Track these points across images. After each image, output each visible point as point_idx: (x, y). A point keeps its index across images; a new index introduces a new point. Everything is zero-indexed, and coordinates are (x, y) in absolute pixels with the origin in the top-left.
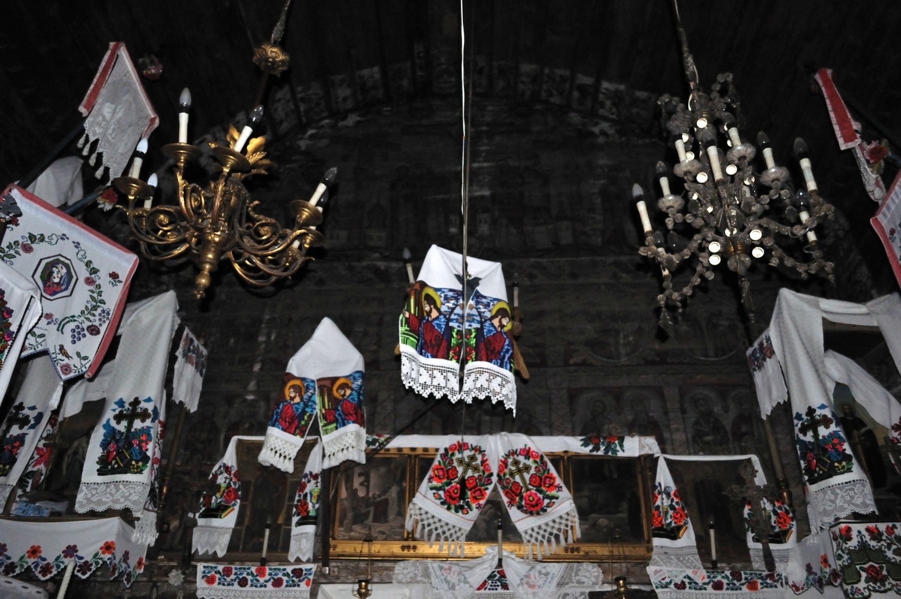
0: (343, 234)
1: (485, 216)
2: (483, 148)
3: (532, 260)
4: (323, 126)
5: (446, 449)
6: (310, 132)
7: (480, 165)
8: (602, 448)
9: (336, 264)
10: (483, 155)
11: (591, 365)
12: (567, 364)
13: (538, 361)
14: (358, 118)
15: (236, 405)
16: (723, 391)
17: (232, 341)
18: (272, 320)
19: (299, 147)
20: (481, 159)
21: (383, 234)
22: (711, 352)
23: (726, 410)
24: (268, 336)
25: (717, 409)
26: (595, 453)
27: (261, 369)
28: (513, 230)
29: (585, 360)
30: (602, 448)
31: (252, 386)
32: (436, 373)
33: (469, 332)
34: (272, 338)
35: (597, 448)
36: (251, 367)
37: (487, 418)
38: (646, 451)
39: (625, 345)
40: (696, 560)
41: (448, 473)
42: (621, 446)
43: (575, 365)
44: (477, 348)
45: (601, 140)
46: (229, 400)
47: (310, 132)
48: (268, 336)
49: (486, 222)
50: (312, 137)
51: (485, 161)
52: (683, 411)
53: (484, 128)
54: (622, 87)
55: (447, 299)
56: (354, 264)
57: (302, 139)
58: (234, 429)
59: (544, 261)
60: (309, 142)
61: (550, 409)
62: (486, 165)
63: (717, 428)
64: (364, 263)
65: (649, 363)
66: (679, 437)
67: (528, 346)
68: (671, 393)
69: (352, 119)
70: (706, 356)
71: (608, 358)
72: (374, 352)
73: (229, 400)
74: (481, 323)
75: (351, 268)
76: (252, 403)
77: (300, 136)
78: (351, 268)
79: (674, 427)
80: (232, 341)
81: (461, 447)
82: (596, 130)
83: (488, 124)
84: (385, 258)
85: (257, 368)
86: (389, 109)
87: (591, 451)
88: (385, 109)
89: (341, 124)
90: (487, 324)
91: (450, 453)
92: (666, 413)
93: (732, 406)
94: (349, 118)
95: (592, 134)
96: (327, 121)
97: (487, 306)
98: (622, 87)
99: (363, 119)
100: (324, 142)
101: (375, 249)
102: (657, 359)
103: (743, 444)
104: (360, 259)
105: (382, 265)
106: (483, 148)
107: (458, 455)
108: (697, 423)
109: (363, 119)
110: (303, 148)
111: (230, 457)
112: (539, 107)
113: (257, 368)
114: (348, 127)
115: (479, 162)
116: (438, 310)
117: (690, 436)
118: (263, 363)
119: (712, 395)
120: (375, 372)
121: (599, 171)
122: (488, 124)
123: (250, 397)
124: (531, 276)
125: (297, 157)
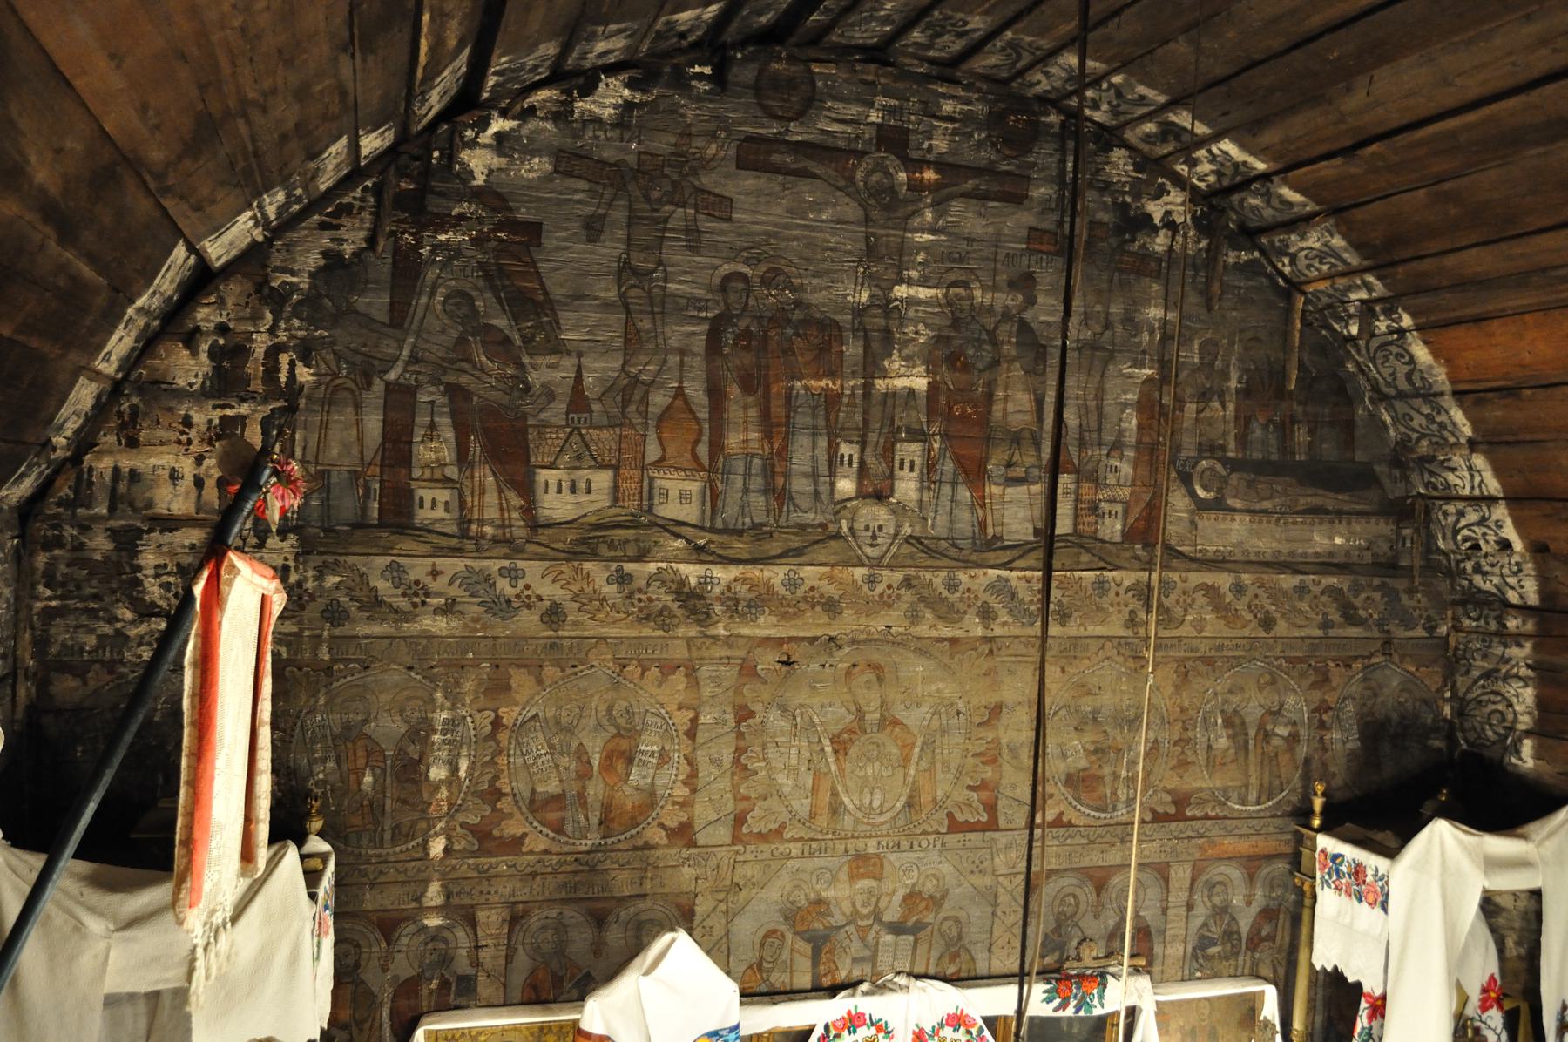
0: (602, 480)
1: (910, 451)
4: (532, 111)
5: (827, 1027)
6: (498, 125)
7: (913, 291)
8: (1073, 1003)
9: (587, 566)
11: (1070, 824)
13: (985, 818)
14: (627, 93)
15: (404, 940)
17: (368, 779)
21: (694, 487)
22: (1253, 796)
26: (1060, 1013)
27: (447, 851)
28: (964, 494)
29: (1062, 813)
30: (1073, 1003)
34: (462, 773)
35: (1063, 1006)
36: (425, 846)
37: (889, 938)
42: (1101, 997)
45: (1160, 242)
46: (388, 926)
47: (498, 125)
50: (499, 136)
51: (924, 282)
53: (930, 175)
56: (629, 567)
57: (473, 144)
61: (994, 914)
62: (923, 293)
66: (1175, 950)
67: (970, 788)
68: (1180, 874)
70: (1244, 802)
71: (1097, 809)
72: (684, 804)
73: (388, 926)
75: (623, 579)
76: (436, 935)
78: (623, 579)
80: (368, 779)
82: (1156, 210)
83: (940, 165)
84: (699, 553)
85: (437, 847)
86: (707, 70)
87: (1055, 1010)
91: (833, 1032)
92: (1164, 911)
93: (1259, 892)
95: (1145, 223)
96: (544, 94)
99: (638, 97)
100: (539, 165)
101: (673, 528)
102: (1172, 810)
103: (1257, 956)
104: (640, 558)
105: (691, 572)
109: (638, 97)
110: (480, 180)
112: (1053, 118)
114: (597, 121)
117: (1189, 949)
120: (686, 853)
121: (1145, 336)
122: (940, 165)
123: (433, 921)
124: (986, 614)
125: (464, 207)
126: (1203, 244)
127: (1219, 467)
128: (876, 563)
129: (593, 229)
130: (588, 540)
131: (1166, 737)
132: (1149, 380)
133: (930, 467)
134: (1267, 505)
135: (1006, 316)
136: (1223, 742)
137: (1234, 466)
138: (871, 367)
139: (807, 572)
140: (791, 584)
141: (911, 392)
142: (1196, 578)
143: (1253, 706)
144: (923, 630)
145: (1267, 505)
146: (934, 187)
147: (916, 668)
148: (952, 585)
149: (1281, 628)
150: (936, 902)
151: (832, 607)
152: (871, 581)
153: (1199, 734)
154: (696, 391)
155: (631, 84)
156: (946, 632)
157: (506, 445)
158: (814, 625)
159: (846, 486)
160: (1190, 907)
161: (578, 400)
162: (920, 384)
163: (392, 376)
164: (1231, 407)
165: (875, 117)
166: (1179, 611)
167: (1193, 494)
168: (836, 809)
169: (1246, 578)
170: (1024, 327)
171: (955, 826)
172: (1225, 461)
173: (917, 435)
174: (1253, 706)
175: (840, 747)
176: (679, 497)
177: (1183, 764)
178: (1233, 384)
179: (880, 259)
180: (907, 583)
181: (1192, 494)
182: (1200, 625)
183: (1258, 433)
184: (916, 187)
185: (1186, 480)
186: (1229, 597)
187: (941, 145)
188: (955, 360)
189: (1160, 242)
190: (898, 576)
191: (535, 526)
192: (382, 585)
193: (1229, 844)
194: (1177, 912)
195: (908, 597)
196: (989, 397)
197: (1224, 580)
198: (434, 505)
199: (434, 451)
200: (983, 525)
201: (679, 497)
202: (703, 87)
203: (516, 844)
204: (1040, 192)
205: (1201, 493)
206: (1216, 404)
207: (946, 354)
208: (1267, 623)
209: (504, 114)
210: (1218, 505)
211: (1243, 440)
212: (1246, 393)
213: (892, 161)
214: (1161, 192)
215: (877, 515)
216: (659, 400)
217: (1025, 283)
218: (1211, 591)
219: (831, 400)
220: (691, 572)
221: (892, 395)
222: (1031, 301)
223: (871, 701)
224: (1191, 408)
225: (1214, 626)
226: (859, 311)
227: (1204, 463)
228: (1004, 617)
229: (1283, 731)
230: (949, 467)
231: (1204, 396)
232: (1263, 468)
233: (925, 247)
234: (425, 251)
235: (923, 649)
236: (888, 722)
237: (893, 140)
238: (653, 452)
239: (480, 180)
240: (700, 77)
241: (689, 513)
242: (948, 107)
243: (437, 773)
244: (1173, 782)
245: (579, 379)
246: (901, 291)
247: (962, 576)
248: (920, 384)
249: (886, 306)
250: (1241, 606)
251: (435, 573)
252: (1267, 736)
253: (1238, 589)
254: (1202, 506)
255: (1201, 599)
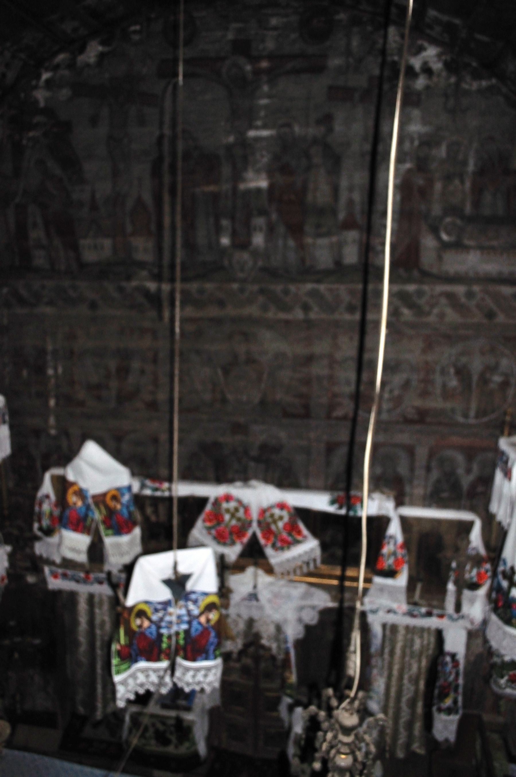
0: (107, 243)
1: (260, 221)
2: (264, 102)
3: (309, 286)
6: (45, 76)
10: (262, 113)
12: (329, 417)
16: (470, 453)
18: (55, 352)
19: (37, 102)
20: (259, 123)
22: (472, 413)
23: (469, 471)
24: (56, 369)
25: (460, 471)
28: (291, 243)
31: (52, 421)
32: (151, 673)
33: (177, 634)
36: (47, 402)
38: (383, 512)
39: (390, 400)
40: (403, 597)
41: (216, 517)
43: (338, 418)
44: (185, 649)
46: (37, 433)
47: (45, 76)
48: (56, 369)
49: (261, 230)
50: (48, 82)
51: (265, 127)
52: (428, 469)
53: (264, 64)
54: (457, 21)
55: (156, 610)
57: (36, 87)
58: (45, 469)
59: (322, 287)
60: (48, 94)
62: (265, 133)
63: (455, 486)
64: (134, 283)
65: (408, 421)
66: (419, 491)
69: (93, 51)
74: (189, 623)
75: (121, 290)
77: (34, 83)
78: (121, 290)
79: (416, 482)
81: (228, 498)
82: (416, 63)
83: (270, 57)
85: (52, 402)
86: (138, 28)
88: (133, 28)
89: (81, 59)
90: (195, 623)
93: (475, 467)
94: (88, 49)
97: (195, 602)
98: (457, 21)
99: (106, 49)
100: (65, 93)
101: (142, 265)
104: (129, 278)
105: (152, 286)
106: (264, 102)
107: (225, 505)
108: (438, 481)
109: (106, 49)
110: (42, 104)
111: (47, 487)
113: (52, 402)
114: (88, 65)
115: (257, 128)
116: (149, 619)
118: (57, 398)
119: (460, 458)
122: (270, 57)
124: (306, 308)
126: (453, 80)
127: (459, 222)
128: (244, 281)
129: (94, 121)
130: (103, 272)
131: (415, 378)
132: (409, 171)
133: (271, 230)
134: (495, 243)
135: (315, 141)
136: (454, 383)
137: (470, 220)
138: (237, 177)
139: (209, 286)
140: (201, 291)
141: (259, 190)
142: (440, 288)
143: (477, 365)
144: (270, 315)
145: (495, 243)
146: (269, 71)
147: (266, 335)
148: (286, 292)
149: (501, 318)
150: (277, 449)
151: (221, 304)
152: (242, 290)
153: (438, 379)
154: (147, 198)
155: (103, 43)
156: (282, 316)
157: (65, 229)
158: (214, 312)
159: (225, 241)
160: (428, 469)
161: (94, 207)
162: (263, 184)
163: (17, 200)
164: (468, 185)
165: (230, 36)
166: (427, 308)
167: (438, 238)
168: (224, 401)
169: (476, 288)
170: (327, 147)
171: (286, 414)
172: (462, 217)
173: (263, 212)
174: (477, 365)
175: (226, 372)
176: (143, 248)
177: (424, 394)
178: (471, 167)
179: (243, 116)
180: (262, 291)
181: (438, 238)
182: (442, 316)
183: (487, 198)
184: (257, 72)
185: (435, 230)
186: (463, 300)
187: (270, 45)
188: (285, 169)
189: (421, 83)
190: (255, 288)
191: (82, 265)
192: (23, 292)
193: (455, 440)
194: (420, 472)
195: (261, 299)
196: (305, 189)
197: (460, 289)
198: (40, 259)
199: (37, 234)
200: (303, 260)
201: (143, 248)
202: (136, 38)
203: (81, 404)
204: (335, 62)
205: (445, 237)
206: (457, 182)
207: (279, 167)
208: (490, 315)
209: (47, 70)
210: (458, 246)
211: (477, 204)
212: (481, 172)
213: (241, 60)
214: (421, 49)
215: (245, 256)
216: (130, 203)
217: (327, 120)
218: (451, 297)
219: (215, 197)
220: (152, 286)
221: (248, 192)
222: (330, 130)
223: (242, 349)
224: (438, 186)
225: (452, 316)
226: (229, 148)
227: (448, 220)
228: (316, 309)
229: (497, 379)
230: (281, 229)
231: (448, 178)
232: (492, 221)
233: (266, 107)
234: (24, 142)
235: (271, 325)
236: (250, 361)
237: (242, 47)
238: (129, 228)
239: (42, 104)
240: (135, 32)
241: (148, 257)
242: (274, 21)
243: (50, 372)
244: (418, 403)
245: (93, 196)
246: (252, 133)
247: (292, 288)
248: (263, 184)
249: (244, 144)
250: (472, 303)
251: (43, 287)
252: (484, 380)
253: (470, 295)
254: (445, 246)
255: (443, 301)
